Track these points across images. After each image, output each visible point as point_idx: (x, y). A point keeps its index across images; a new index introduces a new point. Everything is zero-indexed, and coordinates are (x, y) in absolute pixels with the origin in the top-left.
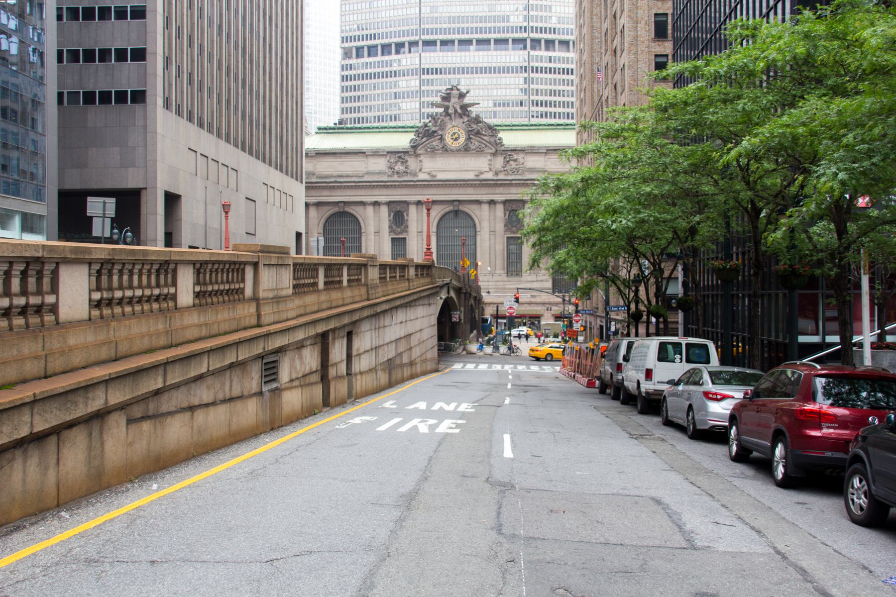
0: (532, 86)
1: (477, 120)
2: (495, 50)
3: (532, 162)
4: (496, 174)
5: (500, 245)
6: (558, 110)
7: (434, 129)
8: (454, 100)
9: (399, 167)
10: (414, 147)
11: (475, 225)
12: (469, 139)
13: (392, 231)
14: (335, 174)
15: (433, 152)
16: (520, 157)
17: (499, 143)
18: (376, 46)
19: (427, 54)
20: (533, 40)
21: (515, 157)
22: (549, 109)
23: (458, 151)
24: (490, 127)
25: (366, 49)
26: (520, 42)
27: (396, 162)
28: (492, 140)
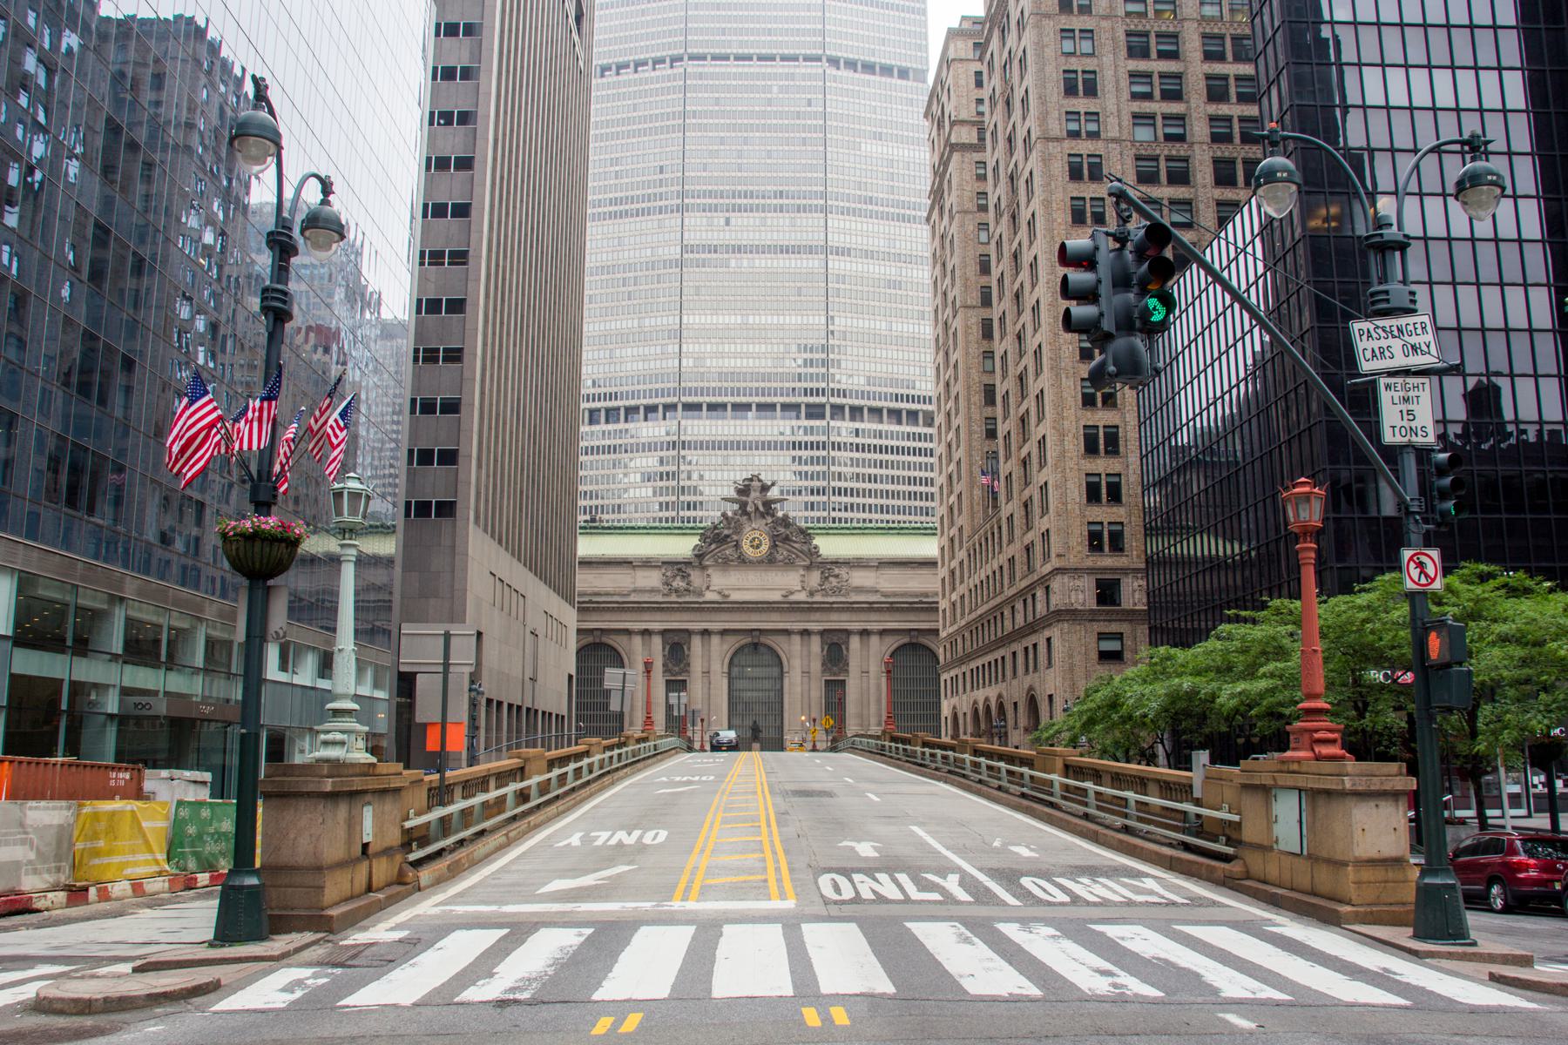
0: (832, 468)
1: (785, 521)
2: (783, 418)
3: (859, 578)
4: (811, 594)
5: (817, 692)
6: (868, 501)
7: (726, 532)
8: (753, 495)
9: (678, 583)
10: (700, 555)
11: (781, 663)
12: (774, 546)
13: (666, 670)
14: (589, 590)
15: (725, 564)
16: (843, 572)
17: (814, 552)
18: (618, 409)
19: (689, 422)
20: (833, 406)
21: (837, 571)
22: (855, 500)
23: (760, 562)
24: (802, 531)
25: (603, 413)
26: (815, 412)
27: (675, 577)
28: (805, 548)
